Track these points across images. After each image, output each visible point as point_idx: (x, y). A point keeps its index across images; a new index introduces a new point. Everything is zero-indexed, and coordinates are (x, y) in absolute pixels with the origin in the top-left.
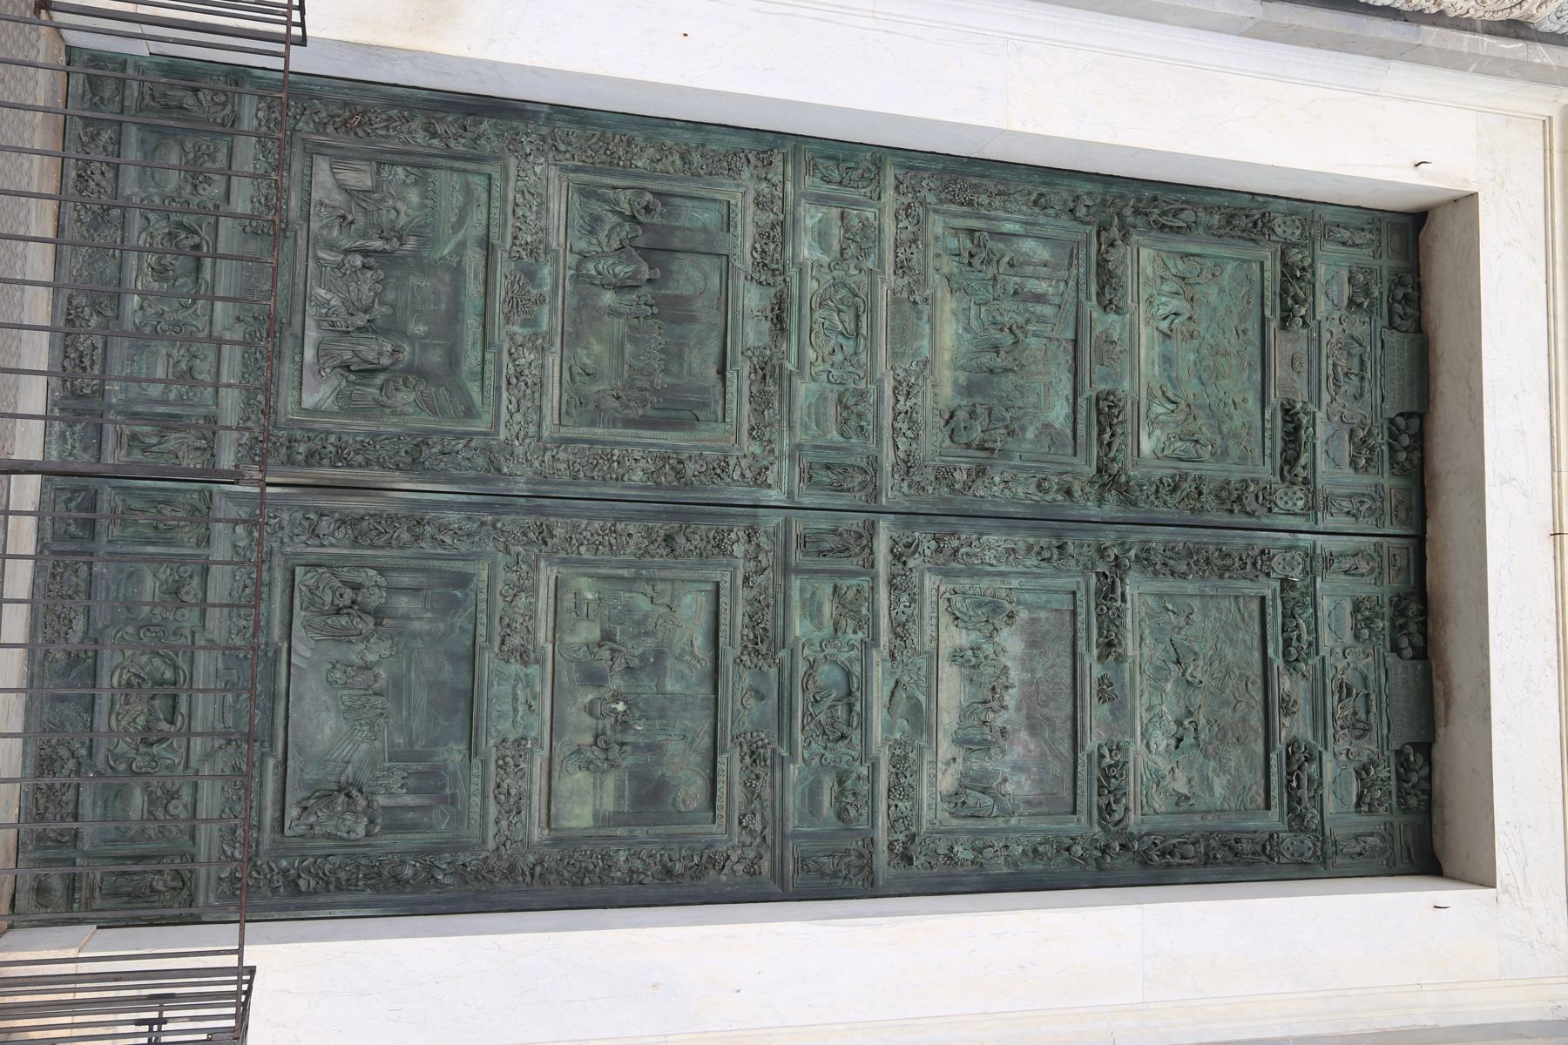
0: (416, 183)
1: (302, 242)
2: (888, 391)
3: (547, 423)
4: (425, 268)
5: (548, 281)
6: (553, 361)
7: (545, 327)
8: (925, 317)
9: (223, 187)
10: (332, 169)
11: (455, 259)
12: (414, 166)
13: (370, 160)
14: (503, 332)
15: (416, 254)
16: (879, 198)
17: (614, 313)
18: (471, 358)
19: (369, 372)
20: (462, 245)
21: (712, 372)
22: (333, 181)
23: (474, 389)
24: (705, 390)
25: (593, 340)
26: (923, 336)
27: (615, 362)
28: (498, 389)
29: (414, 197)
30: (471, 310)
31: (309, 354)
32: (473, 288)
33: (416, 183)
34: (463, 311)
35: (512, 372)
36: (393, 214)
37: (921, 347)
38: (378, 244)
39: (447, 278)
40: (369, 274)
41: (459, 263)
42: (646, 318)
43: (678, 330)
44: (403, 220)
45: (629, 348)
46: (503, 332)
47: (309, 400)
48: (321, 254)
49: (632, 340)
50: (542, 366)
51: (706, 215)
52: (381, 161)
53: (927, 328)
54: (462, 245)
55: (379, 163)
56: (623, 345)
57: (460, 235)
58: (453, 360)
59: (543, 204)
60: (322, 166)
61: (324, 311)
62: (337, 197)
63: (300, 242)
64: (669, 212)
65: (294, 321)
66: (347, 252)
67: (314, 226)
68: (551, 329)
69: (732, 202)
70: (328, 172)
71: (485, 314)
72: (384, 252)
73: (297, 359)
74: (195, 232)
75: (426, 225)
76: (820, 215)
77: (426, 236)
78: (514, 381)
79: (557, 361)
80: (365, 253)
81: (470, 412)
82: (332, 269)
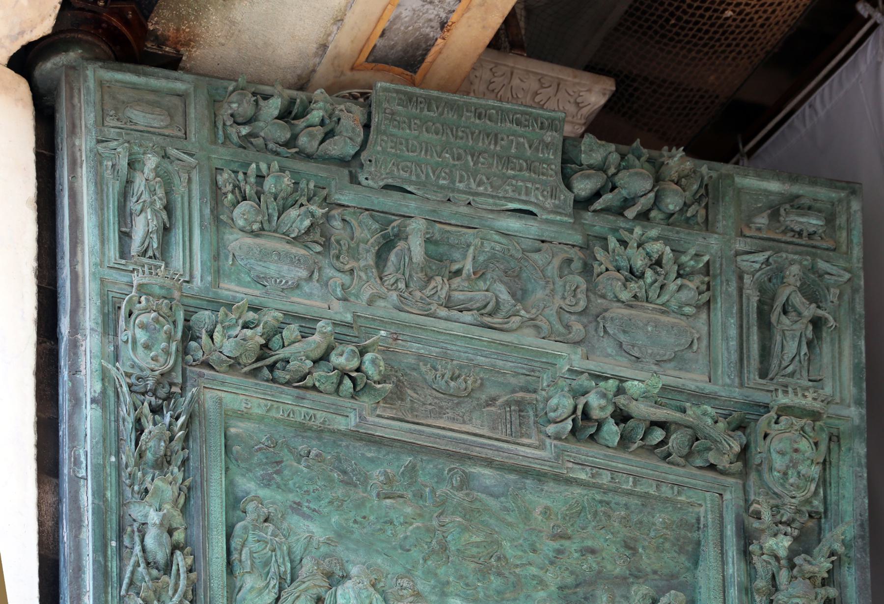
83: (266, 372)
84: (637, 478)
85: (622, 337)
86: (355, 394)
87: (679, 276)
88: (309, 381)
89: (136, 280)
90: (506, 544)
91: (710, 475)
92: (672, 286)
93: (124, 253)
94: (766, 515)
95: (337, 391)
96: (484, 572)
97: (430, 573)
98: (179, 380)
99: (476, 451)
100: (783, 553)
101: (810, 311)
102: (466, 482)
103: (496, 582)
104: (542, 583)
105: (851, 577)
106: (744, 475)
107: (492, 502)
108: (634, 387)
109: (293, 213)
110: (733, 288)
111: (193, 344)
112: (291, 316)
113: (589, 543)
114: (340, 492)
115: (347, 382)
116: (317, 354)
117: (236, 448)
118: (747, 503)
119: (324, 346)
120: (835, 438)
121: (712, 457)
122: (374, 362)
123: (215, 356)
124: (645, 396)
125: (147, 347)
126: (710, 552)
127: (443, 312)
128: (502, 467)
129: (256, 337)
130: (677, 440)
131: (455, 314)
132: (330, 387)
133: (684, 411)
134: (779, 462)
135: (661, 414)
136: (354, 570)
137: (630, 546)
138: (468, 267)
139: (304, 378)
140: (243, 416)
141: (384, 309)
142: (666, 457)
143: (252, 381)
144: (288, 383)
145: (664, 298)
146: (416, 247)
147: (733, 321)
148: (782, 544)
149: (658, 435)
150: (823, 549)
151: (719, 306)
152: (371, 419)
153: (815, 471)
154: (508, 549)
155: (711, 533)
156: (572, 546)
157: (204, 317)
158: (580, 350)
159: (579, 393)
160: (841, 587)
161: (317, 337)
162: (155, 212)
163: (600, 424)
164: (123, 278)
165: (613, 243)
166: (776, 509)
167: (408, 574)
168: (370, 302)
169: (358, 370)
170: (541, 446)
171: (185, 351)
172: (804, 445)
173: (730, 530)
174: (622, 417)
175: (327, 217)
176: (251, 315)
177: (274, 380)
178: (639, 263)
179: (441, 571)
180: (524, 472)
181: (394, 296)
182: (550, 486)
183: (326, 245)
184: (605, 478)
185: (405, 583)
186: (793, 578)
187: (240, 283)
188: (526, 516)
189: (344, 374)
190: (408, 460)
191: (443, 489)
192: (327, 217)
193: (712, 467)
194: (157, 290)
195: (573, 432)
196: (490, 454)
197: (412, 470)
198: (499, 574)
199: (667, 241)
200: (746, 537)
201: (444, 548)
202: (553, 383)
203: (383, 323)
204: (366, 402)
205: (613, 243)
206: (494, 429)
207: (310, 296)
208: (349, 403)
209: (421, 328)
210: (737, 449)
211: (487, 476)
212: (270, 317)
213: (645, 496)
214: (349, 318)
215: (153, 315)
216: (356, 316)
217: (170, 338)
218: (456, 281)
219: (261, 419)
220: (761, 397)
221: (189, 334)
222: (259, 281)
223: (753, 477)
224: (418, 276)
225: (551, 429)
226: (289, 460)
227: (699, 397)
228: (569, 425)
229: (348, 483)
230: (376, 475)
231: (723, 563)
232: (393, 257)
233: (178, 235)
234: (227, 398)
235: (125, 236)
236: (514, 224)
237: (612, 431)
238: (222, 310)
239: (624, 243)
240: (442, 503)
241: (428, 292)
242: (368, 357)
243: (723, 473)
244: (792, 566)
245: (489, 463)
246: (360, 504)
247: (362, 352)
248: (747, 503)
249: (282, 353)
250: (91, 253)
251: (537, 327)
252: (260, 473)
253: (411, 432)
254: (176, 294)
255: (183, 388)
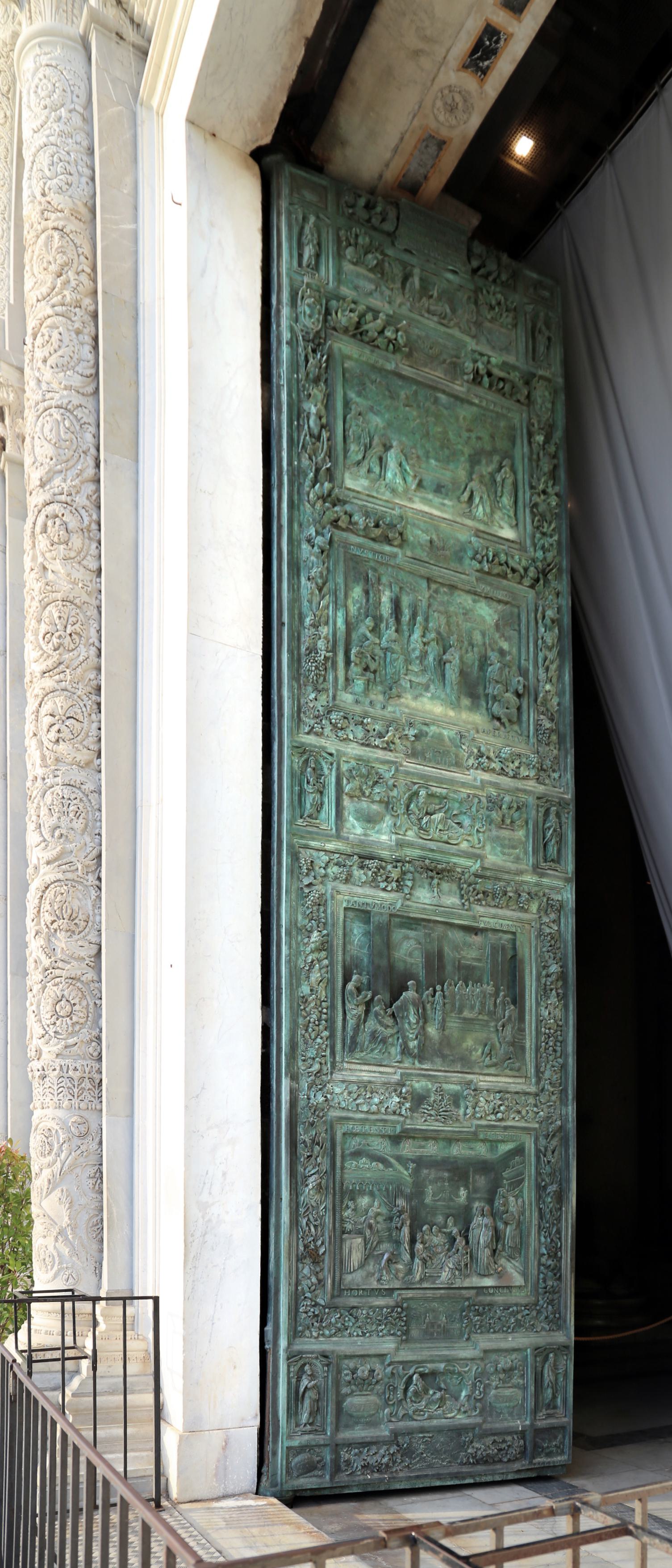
0: (353, 1199)
1: (410, 1294)
2: (486, 776)
3: (526, 1088)
4: (418, 1191)
5: (424, 1083)
6: (484, 1081)
7: (457, 1088)
8: (425, 728)
9: (374, 1359)
10: (351, 1273)
11: (412, 1166)
12: (342, 1202)
13: (342, 1241)
14: (465, 1124)
15: (409, 1198)
16: (331, 755)
17: (443, 1027)
18: (481, 1150)
19: (497, 1236)
20: (399, 1159)
21: (477, 939)
22: (360, 1271)
23: (504, 1148)
24: (494, 948)
25: (464, 1045)
26: (441, 734)
27: (477, 1027)
28: (506, 1128)
29: (364, 1201)
30: (447, 1151)
31: (488, 1282)
32: (432, 1149)
33: (353, 1199)
34: (448, 1158)
35: (493, 1117)
36: (380, 1219)
37: (449, 737)
38: (406, 1230)
39: (425, 1171)
40: (426, 1237)
41: (413, 1161)
42: (444, 997)
43: (449, 968)
44: (384, 1210)
45: (466, 1014)
46: (465, 1124)
47: (518, 1280)
48: (418, 1278)
49: (461, 1011)
50: (488, 1090)
51: (355, 932)
52: (340, 1233)
53: (433, 729)
54: (399, 1159)
55: (343, 1232)
56: (465, 1019)
57: (392, 1161)
58: (484, 1167)
59: (364, 1085)
60: (355, 1278)
61: (457, 1273)
62: (371, 1267)
63: (411, 1295)
64: (357, 967)
65: (468, 1296)
66: (413, 1256)
67: (397, 1284)
68: (460, 1083)
69: (345, 905)
70: (354, 1275)
71: (450, 1140)
72: (411, 1226)
73: (491, 1291)
74: (411, 1377)
75: (387, 1190)
76: (351, 819)
77: (393, 1193)
78: (500, 1115)
79: (481, 1078)
80: (413, 1241)
81: (519, 1151)
82: (426, 1268)
83: (359, 336)
84: (495, 404)
85: (488, 336)
86: (394, 352)
87: (507, 311)
88: (376, 343)
89: (306, 279)
90: (450, 433)
91: (518, 405)
92: (504, 315)
93: (300, 264)
94: (536, 425)
95: (387, 350)
96: (442, 447)
97: (423, 446)
98: (323, 336)
99: (439, 386)
100: (541, 443)
101: (547, 333)
102: (436, 401)
103: (447, 452)
104: (463, 453)
105: (561, 455)
106: (528, 406)
107: (445, 412)
108: (493, 360)
109: (370, 256)
110: (523, 319)
111: (329, 318)
112: (369, 309)
113: (479, 434)
114: (388, 402)
115: (391, 346)
116: (379, 329)
117: (347, 375)
118: (530, 419)
119: (382, 326)
120: (556, 392)
121: (519, 396)
122: (402, 336)
123: (338, 326)
124: (497, 366)
125: (310, 316)
126: (518, 441)
127: (426, 315)
128: (449, 395)
129: (354, 317)
130: (507, 387)
131: (430, 316)
132: (383, 346)
133: (509, 373)
134: (539, 401)
135: (502, 374)
136: (395, 444)
137: (492, 437)
138: (435, 294)
139: (373, 341)
140: (349, 358)
141: (404, 310)
142: (504, 395)
143: (352, 340)
144: (368, 343)
145: (502, 320)
146: (416, 281)
147: (523, 334)
148: (540, 438)
149: (501, 385)
150: (553, 442)
151: (519, 326)
152: (401, 365)
153: (549, 406)
154: (451, 435)
155: (519, 432)
156: (473, 435)
157: (334, 303)
158: (475, 341)
159: (475, 361)
160: (558, 459)
161: (379, 321)
162: (314, 246)
163: (482, 377)
164: (299, 278)
165: (485, 292)
166: (539, 422)
167: (415, 447)
168: (400, 306)
169: (396, 339)
170: (462, 386)
171: (325, 321)
172: (547, 394)
173: (525, 431)
174: (489, 374)
175: (383, 260)
176: (353, 306)
177: (362, 341)
178: (494, 302)
179: (427, 445)
180: (456, 397)
181: (408, 304)
182: (466, 406)
183: (383, 274)
184: (484, 404)
185: (414, 451)
186: (544, 455)
187: (348, 288)
188: (457, 419)
189: (390, 341)
190: (414, 388)
191: (428, 404)
192: (383, 260)
193: (518, 401)
194: (314, 287)
195: (474, 379)
196: (444, 387)
197: (416, 393)
198: (448, 448)
199: (502, 294)
200: (530, 435)
201: (428, 434)
202: (466, 356)
203: (405, 318)
204: (398, 356)
205: (485, 292)
206: (445, 375)
207: (376, 299)
208: (390, 356)
209: (418, 321)
210: (526, 393)
211: (443, 397)
212: (361, 308)
213: (497, 413)
214: (391, 312)
215: (312, 300)
216: (394, 312)
217: (319, 313)
218: (431, 301)
219: (357, 361)
220: (533, 370)
221: (328, 312)
222: (356, 288)
223: (531, 407)
224: (417, 296)
225: (466, 377)
226: (368, 384)
227: (514, 368)
228: (472, 376)
229: (392, 398)
230: (402, 394)
231: (523, 446)
232: (408, 285)
233: (323, 259)
234: (343, 348)
235: (300, 256)
236: (450, 276)
237: (486, 380)
238: (341, 302)
239: (488, 292)
240: (427, 411)
241: (421, 304)
242: (400, 333)
243: (522, 404)
244: (544, 449)
245: (444, 392)
246: (396, 409)
247: (397, 331)
248: (530, 419)
249: (365, 327)
250: (286, 262)
251: (460, 328)
252: (357, 389)
253: (416, 374)
254: (322, 290)
255: (325, 340)
